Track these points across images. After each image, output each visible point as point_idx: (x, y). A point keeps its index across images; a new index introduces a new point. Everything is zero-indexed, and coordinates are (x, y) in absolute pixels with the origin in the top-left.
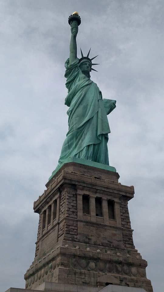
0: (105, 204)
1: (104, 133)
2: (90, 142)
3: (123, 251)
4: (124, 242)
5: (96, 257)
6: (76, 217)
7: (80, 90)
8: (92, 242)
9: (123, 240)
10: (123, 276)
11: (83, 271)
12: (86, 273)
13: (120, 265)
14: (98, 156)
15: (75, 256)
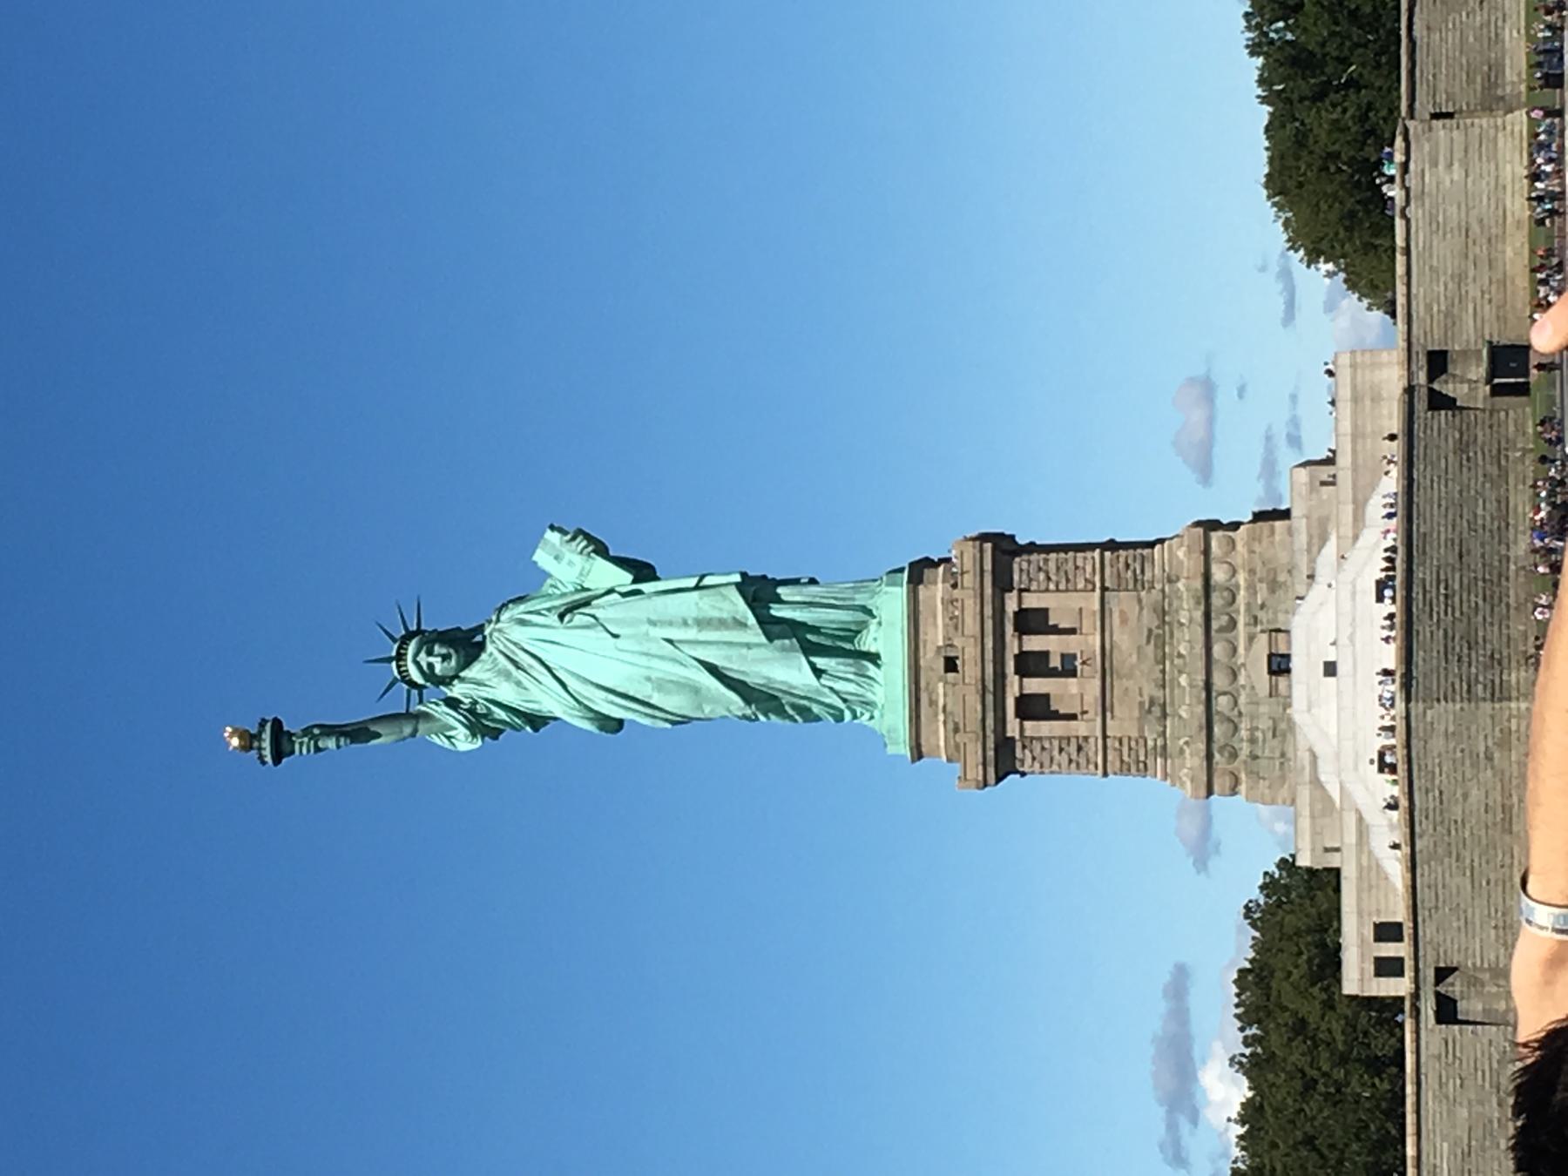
0: (1034, 643)
1: (752, 620)
2: (800, 670)
3: (1169, 597)
4: (1139, 587)
5: (1203, 695)
6: (1092, 740)
7: (587, 707)
8: (1158, 694)
9: (1135, 589)
10: (1242, 609)
11: (1244, 734)
12: (1249, 727)
13: (1213, 615)
14: (834, 626)
15: (1209, 757)
